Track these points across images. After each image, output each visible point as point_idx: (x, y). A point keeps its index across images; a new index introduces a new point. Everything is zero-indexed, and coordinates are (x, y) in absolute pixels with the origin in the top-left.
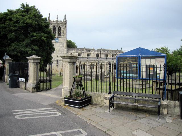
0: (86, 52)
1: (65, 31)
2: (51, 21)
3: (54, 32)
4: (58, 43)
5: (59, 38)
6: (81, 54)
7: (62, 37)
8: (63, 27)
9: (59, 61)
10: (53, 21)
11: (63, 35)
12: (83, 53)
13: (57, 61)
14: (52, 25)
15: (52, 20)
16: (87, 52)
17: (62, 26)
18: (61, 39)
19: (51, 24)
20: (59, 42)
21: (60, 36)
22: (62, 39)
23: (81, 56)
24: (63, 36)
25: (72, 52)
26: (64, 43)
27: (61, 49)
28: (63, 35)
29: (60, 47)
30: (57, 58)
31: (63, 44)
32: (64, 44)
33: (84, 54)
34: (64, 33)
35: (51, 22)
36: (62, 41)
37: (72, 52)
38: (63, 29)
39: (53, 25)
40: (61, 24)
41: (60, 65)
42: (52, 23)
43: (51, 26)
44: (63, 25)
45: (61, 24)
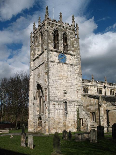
1: (75, 42)
2: (51, 20)
3: (56, 42)
4: (65, 65)
5: (66, 55)
7: (72, 53)
8: (71, 36)
9: (68, 104)
10: (55, 21)
11: (73, 49)
12: (105, 87)
14: (52, 27)
15: (53, 19)
16: (110, 86)
17: (70, 34)
19: (51, 25)
21: (67, 50)
22: (72, 57)
24: (73, 51)
25: (88, 84)
26: (75, 65)
27: (72, 76)
28: (73, 49)
30: (65, 96)
31: (74, 67)
32: (76, 66)
34: (73, 47)
35: (50, 22)
36: (71, 62)
37: (88, 84)
38: (72, 38)
39: (54, 28)
40: (68, 29)
41: (71, 113)
42: (52, 24)
43: (52, 30)
44: (72, 31)
45: (68, 29)
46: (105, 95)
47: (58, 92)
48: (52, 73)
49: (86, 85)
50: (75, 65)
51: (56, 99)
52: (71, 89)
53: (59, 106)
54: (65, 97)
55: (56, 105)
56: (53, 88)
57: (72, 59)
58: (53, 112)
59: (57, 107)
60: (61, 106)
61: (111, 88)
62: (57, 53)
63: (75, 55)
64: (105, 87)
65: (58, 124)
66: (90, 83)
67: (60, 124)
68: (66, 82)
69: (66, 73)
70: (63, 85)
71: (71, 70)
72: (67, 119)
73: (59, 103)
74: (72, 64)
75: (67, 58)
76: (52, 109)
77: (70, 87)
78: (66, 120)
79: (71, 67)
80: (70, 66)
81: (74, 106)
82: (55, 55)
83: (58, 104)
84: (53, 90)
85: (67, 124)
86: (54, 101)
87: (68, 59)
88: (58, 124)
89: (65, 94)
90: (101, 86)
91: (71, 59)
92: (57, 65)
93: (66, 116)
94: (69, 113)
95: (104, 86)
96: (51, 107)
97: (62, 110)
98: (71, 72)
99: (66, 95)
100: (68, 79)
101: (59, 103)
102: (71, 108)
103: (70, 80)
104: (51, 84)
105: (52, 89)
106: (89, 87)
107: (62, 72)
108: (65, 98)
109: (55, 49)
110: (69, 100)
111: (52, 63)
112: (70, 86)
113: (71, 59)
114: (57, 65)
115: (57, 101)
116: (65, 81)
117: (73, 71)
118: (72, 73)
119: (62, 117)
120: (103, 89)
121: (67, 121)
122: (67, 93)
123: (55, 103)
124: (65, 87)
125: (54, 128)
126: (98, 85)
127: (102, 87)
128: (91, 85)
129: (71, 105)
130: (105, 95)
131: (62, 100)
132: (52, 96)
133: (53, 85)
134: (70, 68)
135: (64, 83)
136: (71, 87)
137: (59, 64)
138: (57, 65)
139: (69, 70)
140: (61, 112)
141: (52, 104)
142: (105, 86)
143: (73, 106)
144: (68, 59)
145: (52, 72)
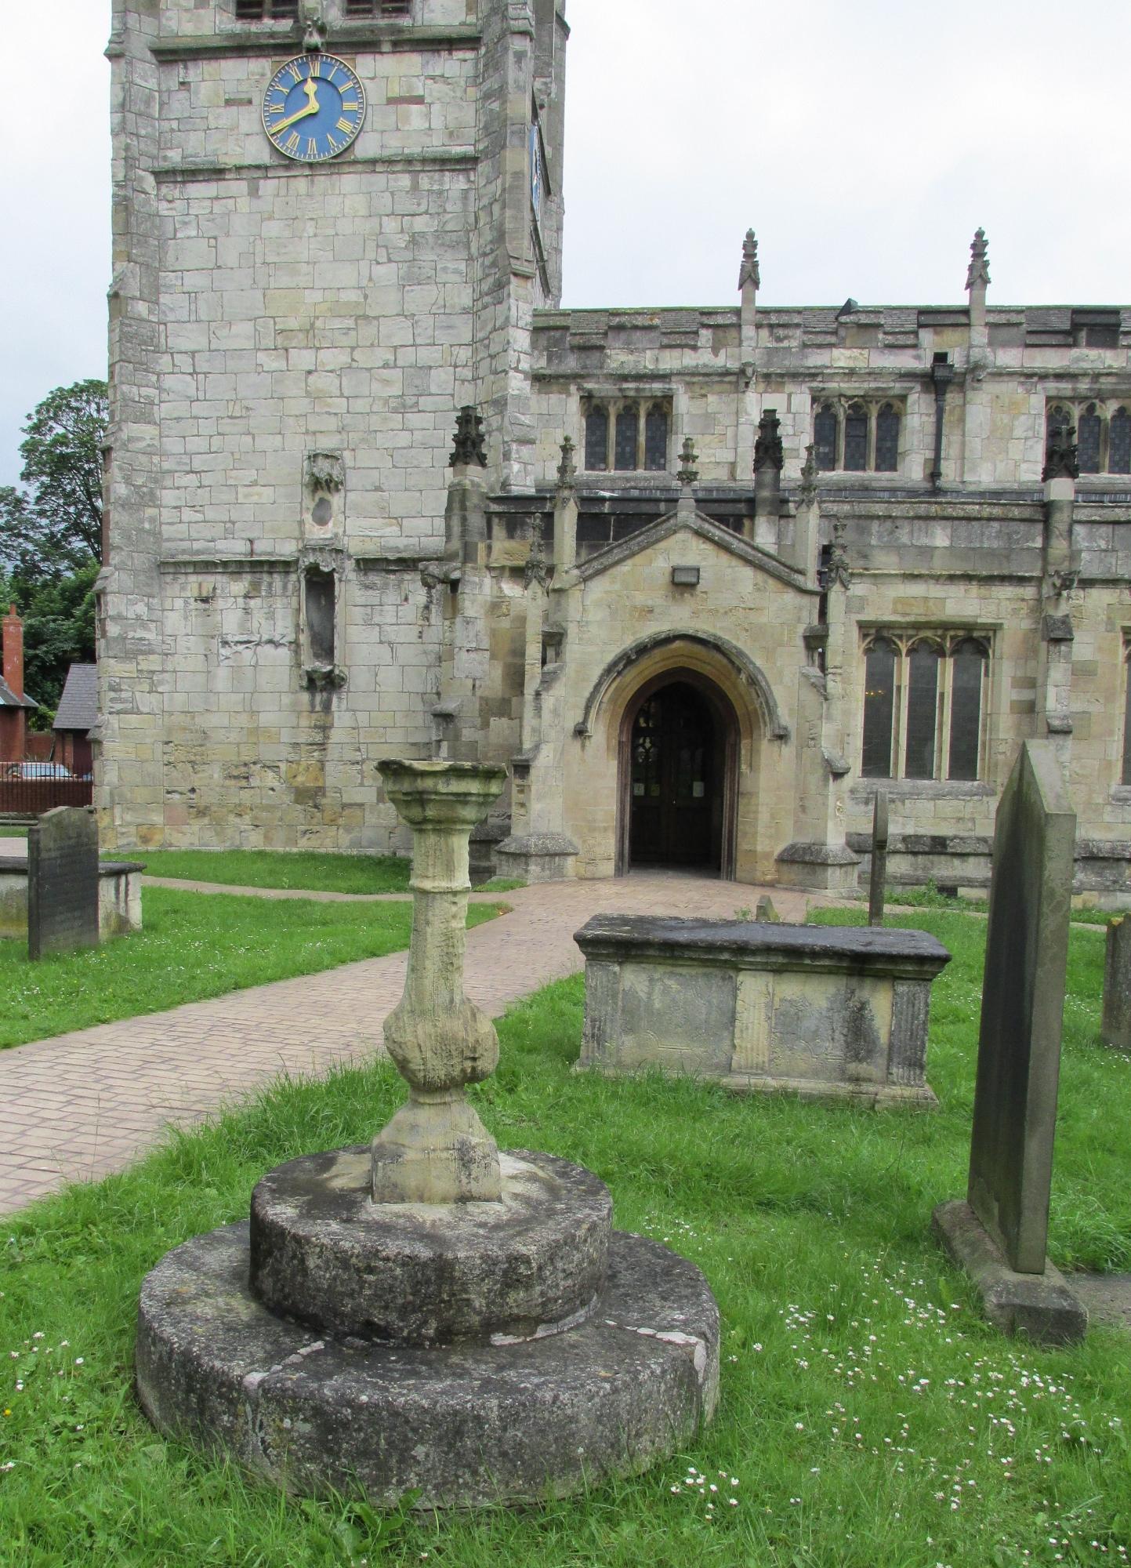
0: (1010, 358)
4: (349, 181)
5: (365, 66)
6: (892, 415)
9: (350, 591)
13: (321, 585)
18: (412, 62)
20: (366, 148)
23: (889, 458)
25: (671, 361)
26: (466, 163)
27: (421, 298)
29: (387, 273)
30: (321, 521)
32: (482, 167)
33: (980, 408)
37: (671, 361)
46: (934, 475)
47: (251, 475)
48: (192, 295)
49: (625, 378)
50: (466, 163)
51: (221, 545)
52: (404, 439)
53: (258, 617)
54: (321, 521)
55: (220, 603)
56: (195, 444)
57: (431, 90)
58: (197, 663)
59: (229, 618)
60: (271, 616)
61: (1052, 387)
62: (260, 67)
63: (470, 42)
64: (939, 380)
65: (241, 775)
66: (694, 348)
67: (254, 782)
68: (340, 372)
69: (347, 275)
70: (302, 405)
71: (420, 224)
72: (336, 735)
73: (255, 586)
74: (437, 145)
75: (374, 93)
76: (182, 643)
77: (395, 411)
78: (322, 746)
79: (415, 187)
80: (405, 181)
81: (427, 607)
82: (231, 89)
83: (246, 597)
84: (197, 464)
85: (330, 782)
86: (207, 567)
87: (391, 101)
88: (241, 775)
89: (320, 494)
90: (872, 374)
91: (419, 100)
92: (254, 192)
93: (327, 707)
94: (358, 679)
95: (940, 358)
96: (174, 621)
97: (284, 654)
98: (415, 241)
99: (336, 500)
100: (367, 332)
101: (255, 586)
102: (392, 633)
103: (396, 342)
104: (182, 408)
105: (190, 448)
106: (683, 404)
107: (304, 268)
108: (318, 534)
109: (239, 26)
110: (372, 550)
111: (196, 190)
112: (386, 401)
113: (419, 100)
114: (244, 204)
115: (234, 568)
116: (334, 358)
117: (440, 234)
118: (427, 256)
119: (280, 705)
120: (913, 398)
121: (333, 753)
122: (352, 479)
123: (209, 581)
124: (332, 424)
125: (202, 812)
126: (816, 359)
127: (897, 387)
128: (722, 361)
129: (392, 597)
130: (934, 475)
131: (287, 549)
132: (188, 515)
133: (198, 409)
134: (407, 205)
135: (322, 382)
136: (402, 409)
137: (268, 187)
138: (254, 192)
139: (391, 225)
140: (278, 669)
141: (183, 589)
142: (956, 359)
143: (410, 612)
144: (391, 101)
145: (192, 281)
